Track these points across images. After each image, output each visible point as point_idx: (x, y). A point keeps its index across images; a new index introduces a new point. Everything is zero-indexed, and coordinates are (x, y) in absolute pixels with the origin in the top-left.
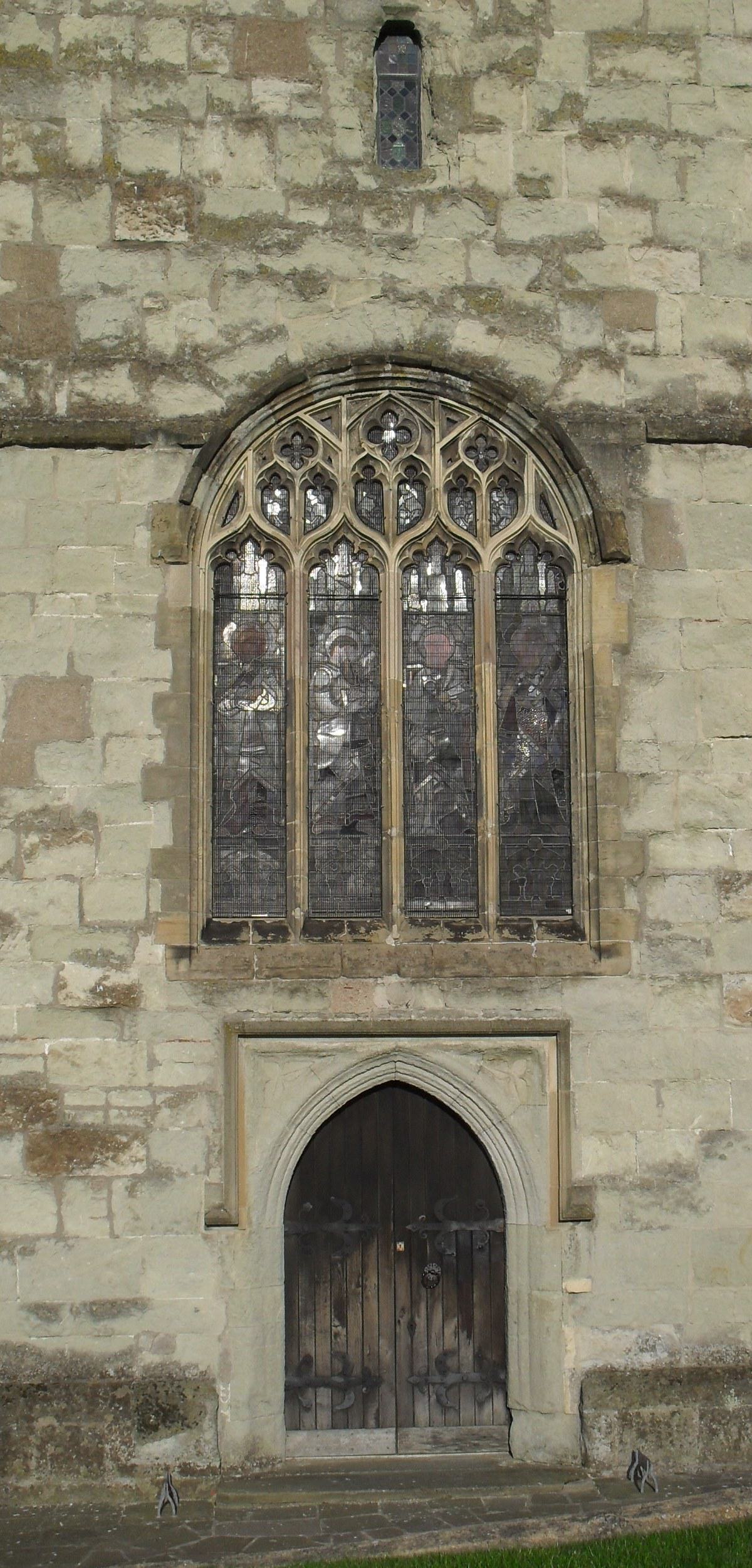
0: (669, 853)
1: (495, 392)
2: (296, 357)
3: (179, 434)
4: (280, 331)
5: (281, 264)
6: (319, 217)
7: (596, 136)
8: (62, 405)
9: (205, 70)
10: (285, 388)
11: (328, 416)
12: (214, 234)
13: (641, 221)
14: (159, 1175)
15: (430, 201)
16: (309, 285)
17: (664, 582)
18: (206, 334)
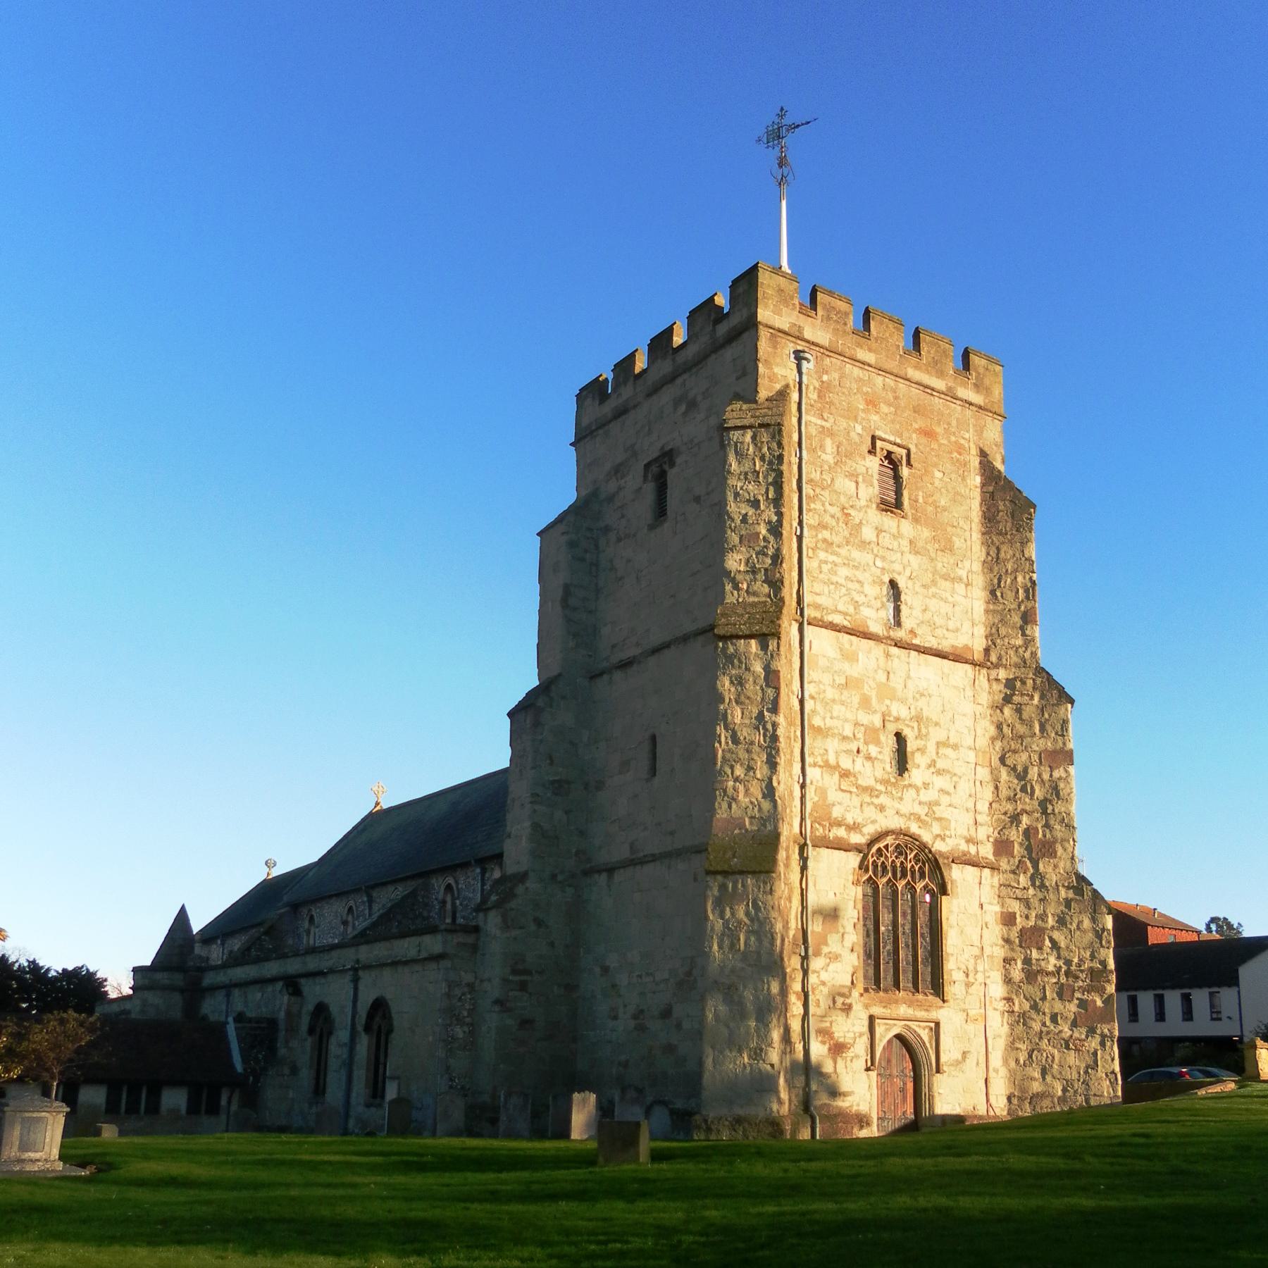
1: (923, 847)
3: (857, 849)
5: (876, 801)
6: (882, 788)
7: (939, 772)
8: (831, 835)
14: (857, 1056)
16: (882, 808)
17: (955, 902)
18: (859, 820)
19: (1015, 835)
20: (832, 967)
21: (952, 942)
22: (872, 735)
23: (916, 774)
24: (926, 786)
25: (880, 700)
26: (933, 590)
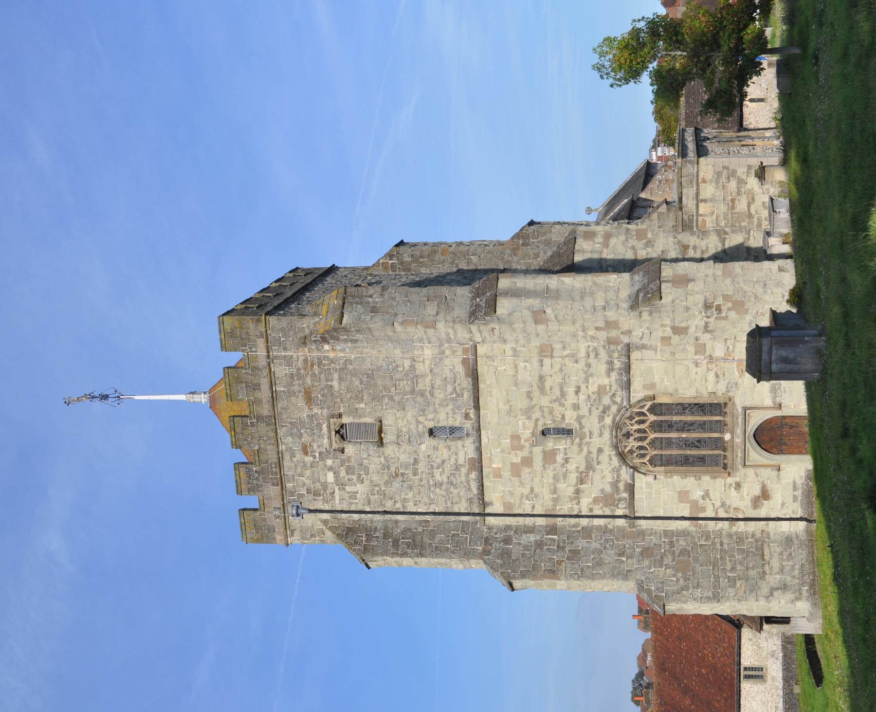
0: (711, 388)
2: (614, 453)
4: (610, 455)
9: (555, 470)
10: (622, 456)
11: (626, 446)
12: (589, 467)
13: (583, 387)
15: (582, 427)
16: (600, 450)
19: (603, 335)
20: (712, 497)
21: (688, 393)
22: (549, 457)
23: (570, 420)
24: (576, 407)
25: (521, 448)
26: (428, 394)
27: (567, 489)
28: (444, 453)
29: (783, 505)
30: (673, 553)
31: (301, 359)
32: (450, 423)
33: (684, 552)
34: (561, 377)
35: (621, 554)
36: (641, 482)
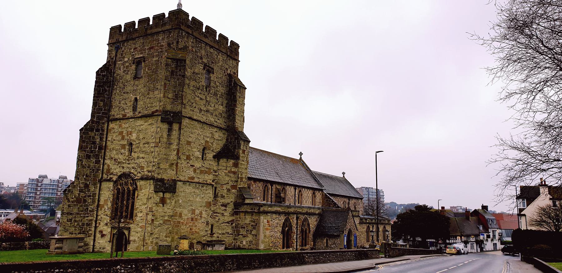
16: (123, 168)
21: (138, 204)
22: (123, 146)
24: (138, 158)
27: (114, 154)
28: (129, 105)
29: (99, 243)
30: (85, 197)
31: (164, 44)
32: (139, 106)
33: (85, 201)
34: (149, 151)
35: (87, 176)
36: (111, 185)
